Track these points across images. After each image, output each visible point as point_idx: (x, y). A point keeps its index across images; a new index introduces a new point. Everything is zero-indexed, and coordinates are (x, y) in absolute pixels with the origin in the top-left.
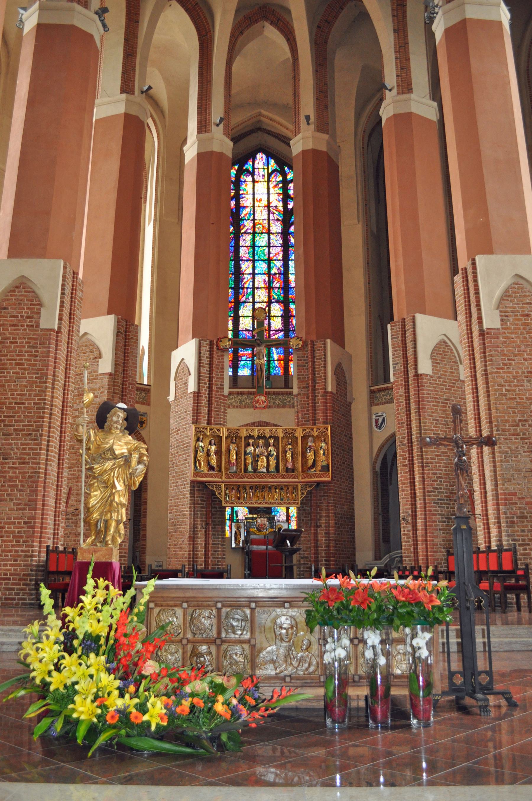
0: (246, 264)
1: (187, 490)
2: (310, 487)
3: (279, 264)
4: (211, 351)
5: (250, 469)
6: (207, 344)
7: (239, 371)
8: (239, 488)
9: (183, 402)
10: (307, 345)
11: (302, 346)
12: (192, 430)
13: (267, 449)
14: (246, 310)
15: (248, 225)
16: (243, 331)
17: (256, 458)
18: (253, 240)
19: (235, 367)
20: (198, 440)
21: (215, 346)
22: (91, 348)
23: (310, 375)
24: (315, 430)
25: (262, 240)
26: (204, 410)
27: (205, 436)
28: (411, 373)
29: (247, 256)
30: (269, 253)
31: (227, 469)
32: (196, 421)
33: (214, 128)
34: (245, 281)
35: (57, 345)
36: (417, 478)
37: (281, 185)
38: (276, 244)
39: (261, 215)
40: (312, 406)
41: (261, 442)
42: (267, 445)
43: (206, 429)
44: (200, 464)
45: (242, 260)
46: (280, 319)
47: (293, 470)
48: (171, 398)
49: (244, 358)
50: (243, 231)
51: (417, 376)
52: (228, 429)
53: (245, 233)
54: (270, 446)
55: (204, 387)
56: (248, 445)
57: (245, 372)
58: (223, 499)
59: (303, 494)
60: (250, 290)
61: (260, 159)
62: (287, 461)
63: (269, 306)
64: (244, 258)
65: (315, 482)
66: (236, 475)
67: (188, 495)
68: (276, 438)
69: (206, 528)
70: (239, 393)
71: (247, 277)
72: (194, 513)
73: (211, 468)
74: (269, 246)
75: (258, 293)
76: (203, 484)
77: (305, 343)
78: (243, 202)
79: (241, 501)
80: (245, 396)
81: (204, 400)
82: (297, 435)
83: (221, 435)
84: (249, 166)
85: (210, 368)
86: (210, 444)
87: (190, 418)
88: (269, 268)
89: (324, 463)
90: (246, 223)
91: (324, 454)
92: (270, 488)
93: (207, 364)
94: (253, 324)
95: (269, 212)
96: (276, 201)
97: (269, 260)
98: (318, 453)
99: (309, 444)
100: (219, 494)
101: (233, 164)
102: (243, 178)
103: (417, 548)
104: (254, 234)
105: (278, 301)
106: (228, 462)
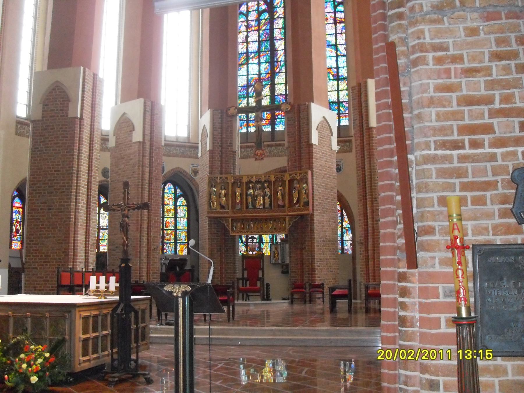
0: (279, 42)
2: (295, 218)
5: (250, 206)
6: (219, 113)
7: (276, 127)
8: (243, 220)
10: (294, 108)
11: (291, 109)
13: (263, 191)
16: (278, 95)
17: (254, 198)
21: (225, 115)
22: (128, 124)
23: (297, 132)
24: (298, 174)
29: (280, 35)
31: (233, 207)
34: (278, 56)
35: (80, 128)
40: (298, 156)
41: (258, 186)
42: (263, 188)
43: (217, 178)
44: (213, 204)
45: (276, 39)
47: (283, 206)
49: (280, 116)
52: (234, 177)
54: (265, 188)
55: (216, 146)
56: (248, 188)
58: (230, 230)
59: (290, 224)
60: (282, 63)
62: (278, 199)
64: (278, 38)
65: (298, 215)
67: (207, 227)
68: (269, 182)
73: (222, 207)
77: (292, 107)
79: (245, 231)
80: (273, 148)
81: (217, 156)
82: (285, 179)
83: (229, 181)
85: (221, 131)
86: (221, 189)
89: (306, 200)
91: (305, 193)
93: (219, 128)
94: (286, 89)
98: (301, 192)
99: (295, 186)
100: (228, 226)
103: (368, 264)
106: (234, 203)
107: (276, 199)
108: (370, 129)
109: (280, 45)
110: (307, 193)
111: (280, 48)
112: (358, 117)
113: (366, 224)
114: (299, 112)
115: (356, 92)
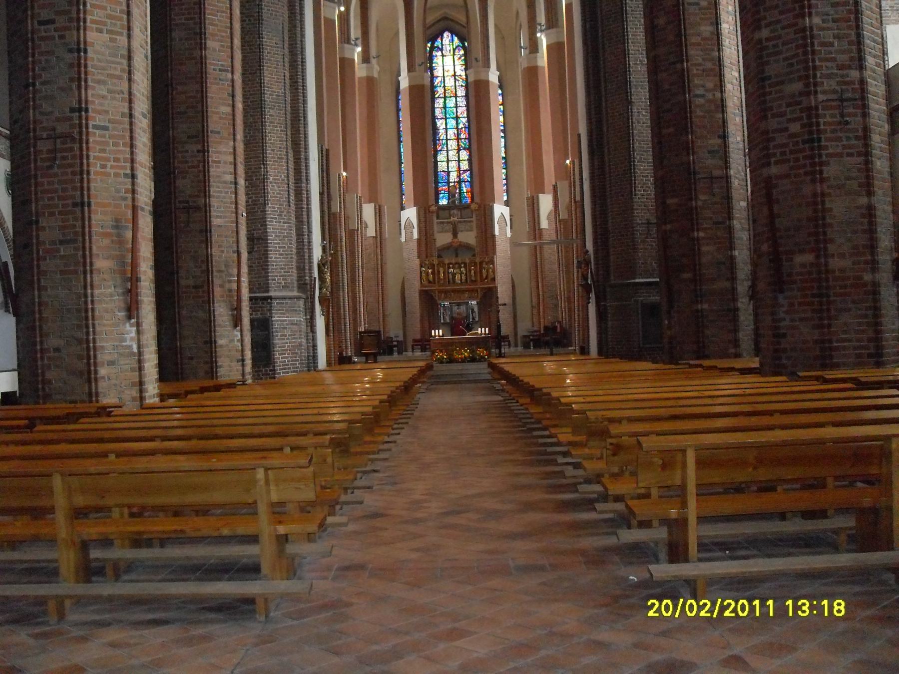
0: (441, 121)
1: (417, 295)
3: (464, 120)
4: (425, 213)
8: (446, 292)
9: (411, 244)
12: (417, 262)
14: (441, 157)
15: (440, 91)
17: (454, 275)
18: (445, 103)
19: (437, 199)
20: (421, 266)
25: (451, 103)
27: (425, 264)
28: (537, 228)
30: (457, 112)
32: (419, 257)
33: (417, 68)
36: (540, 285)
37: (463, 58)
38: (461, 105)
39: (450, 82)
41: (457, 266)
46: (467, 162)
47: (475, 281)
48: (403, 239)
50: (436, 96)
53: (438, 97)
56: (449, 268)
57: (443, 202)
60: (444, 141)
63: (458, 152)
66: (443, 285)
68: (465, 264)
71: (442, 132)
74: (456, 107)
75: (450, 143)
76: (426, 291)
77: (480, 206)
78: (436, 73)
87: (416, 254)
88: (457, 124)
90: (438, 89)
92: (463, 291)
95: (455, 79)
96: (460, 71)
97: (457, 118)
104: (445, 97)
105: (464, 149)
106: (439, 278)
107: (471, 276)
108: (540, 230)
109: (441, 124)
110: (494, 272)
111: (441, 127)
113: (539, 295)
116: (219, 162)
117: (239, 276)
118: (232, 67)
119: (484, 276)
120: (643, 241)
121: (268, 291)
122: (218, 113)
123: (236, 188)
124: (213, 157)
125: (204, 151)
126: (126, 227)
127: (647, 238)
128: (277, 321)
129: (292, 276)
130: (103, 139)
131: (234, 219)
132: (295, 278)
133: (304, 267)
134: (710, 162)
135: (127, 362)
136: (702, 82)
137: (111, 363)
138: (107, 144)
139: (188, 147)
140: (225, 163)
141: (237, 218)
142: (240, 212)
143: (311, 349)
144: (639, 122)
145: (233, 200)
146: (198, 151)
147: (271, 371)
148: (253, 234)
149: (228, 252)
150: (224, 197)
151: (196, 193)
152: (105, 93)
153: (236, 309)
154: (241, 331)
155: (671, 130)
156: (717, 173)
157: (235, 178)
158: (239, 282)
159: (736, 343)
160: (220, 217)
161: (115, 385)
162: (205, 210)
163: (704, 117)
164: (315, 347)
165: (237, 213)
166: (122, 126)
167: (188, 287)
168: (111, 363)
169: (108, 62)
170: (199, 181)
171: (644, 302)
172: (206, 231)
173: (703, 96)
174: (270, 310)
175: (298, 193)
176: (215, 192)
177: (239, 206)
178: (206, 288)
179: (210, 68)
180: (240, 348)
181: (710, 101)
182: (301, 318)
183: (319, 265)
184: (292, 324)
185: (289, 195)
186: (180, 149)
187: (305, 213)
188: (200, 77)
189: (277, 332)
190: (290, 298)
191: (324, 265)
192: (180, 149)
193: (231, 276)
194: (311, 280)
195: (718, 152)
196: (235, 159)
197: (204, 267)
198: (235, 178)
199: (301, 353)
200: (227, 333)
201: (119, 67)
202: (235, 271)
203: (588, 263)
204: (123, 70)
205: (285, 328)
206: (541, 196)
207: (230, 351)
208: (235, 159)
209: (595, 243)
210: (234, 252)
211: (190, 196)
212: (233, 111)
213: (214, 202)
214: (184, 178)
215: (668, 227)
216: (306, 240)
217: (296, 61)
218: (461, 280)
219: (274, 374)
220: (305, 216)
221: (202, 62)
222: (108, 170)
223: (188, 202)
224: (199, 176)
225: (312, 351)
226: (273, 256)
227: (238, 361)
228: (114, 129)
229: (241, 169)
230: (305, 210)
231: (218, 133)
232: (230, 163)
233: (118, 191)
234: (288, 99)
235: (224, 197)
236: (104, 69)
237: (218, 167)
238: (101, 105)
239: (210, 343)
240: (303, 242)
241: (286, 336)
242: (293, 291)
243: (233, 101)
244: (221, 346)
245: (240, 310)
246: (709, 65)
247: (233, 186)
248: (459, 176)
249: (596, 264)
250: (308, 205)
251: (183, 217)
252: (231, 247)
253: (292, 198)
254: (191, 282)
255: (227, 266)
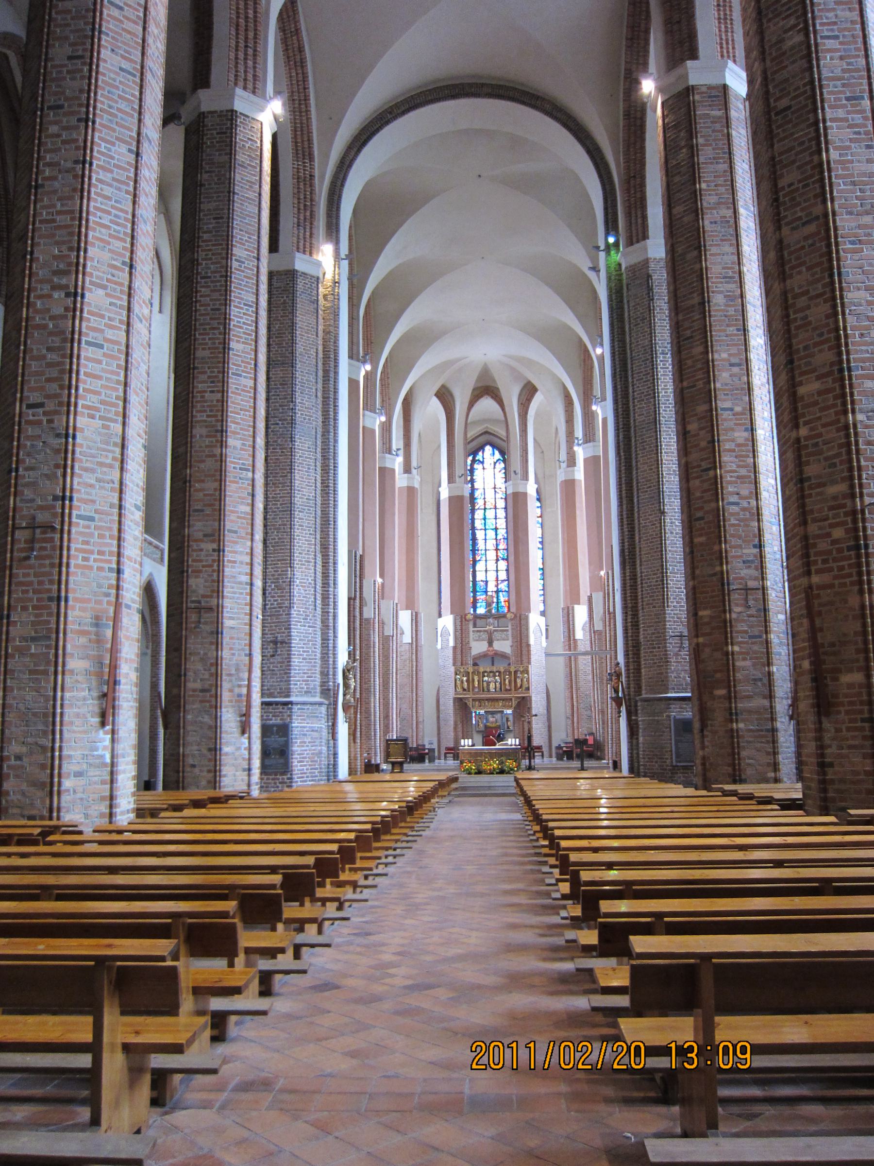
1: (451, 702)
4: (461, 621)
12: (452, 669)
14: (480, 566)
15: (480, 503)
17: (488, 683)
19: (475, 608)
20: (456, 674)
25: (490, 514)
26: (459, 657)
32: (454, 664)
41: (491, 674)
47: (510, 690)
48: (439, 646)
51: (575, 640)
56: (484, 676)
57: (481, 610)
60: (483, 552)
61: (488, 449)
66: (478, 693)
68: (500, 672)
69: (462, 722)
70: (478, 631)
72: (455, 714)
76: (461, 699)
77: (515, 616)
78: (476, 485)
84: (479, 457)
87: (451, 661)
88: (496, 535)
101: (469, 455)
102: (476, 466)
105: (503, 559)
108: (575, 641)
112: (566, 630)
113: (573, 705)
114: (520, 620)
115: (566, 611)
116: (235, 562)
117: (249, 680)
118: (254, 466)
119: (519, 685)
120: (677, 655)
121: (288, 696)
122: (237, 512)
123: (251, 589)
124: (228, 556)
125: (219, 550)
126: (107, 626)
127: (680, 651)
128: (297, 727)
129: (315, 681)
130: (87, 531)
131: (248, 621)
132: (318, 683)
133: (328, 671)
134: (744, 572)
135: (97, 773)
136: (736, 489)
137: (79, 774)
138: (91, 535)
139: (203, 546)
140: (241, 563)
141: (251, 620)
142: (254, 614)
143: (332, 757)
144: (672, 533)
145: (248, 601)
146: (214, 550)
147: (288, 779)
148: (277, 637)
149: (239, 655)
150: (238, 598)
151: (209, 594)
152: (93, 482)
153: (244, 715)
154: (249, 738)
155: (702, 539)
156: (751, 584)
157: (251, 579)
158: (249, 686)
159: (775, 767)
160: (232, 618)
161: (82, 799)
162: (216, 611)
163: (739, 525)
164: (335, 755)
165: (251, 615)
166: (109, 517)
167: (194, 690)
168: (79, 774)
169: (98, 449)
170: (213, 581)
171: (678, 717)
172: (217, 632)
173: (737, 504)
174: (290, 716)
175: (325, 598)
176: (228, 592)
177: (254, 608)
178: (213, 692)
179: (230, 467)
180: (247, 757)
181: (744, 509)
182: (322, 725)
183: (344, 671)
184: (313, 731)
185: (315, 599)
186: (195, 547)
187: (331, 618)
188: (219, 475)
189: (296, 738)
190: (312, 704)
191: (349, 671)
192: (195, 547)
193: (243, 680)
194: (334, 686)
195: (752, 562)
196: (252, 559)
197: (213, 670)
198: (251, 579)
199: (321, 761)
200: (234, 740)
201: (110, 455)
202: (246, 675)
203: (619, 675)
204: (114, 459)
205: (305, 735)
206: (576, 607)
207: (236, 759)
208: (252, 559)
209: (626, 655)
210: (246, 655)
211: (203, 596)
212: (253, 510)
213: (227, 603)
214: (197, 577)
215: (701, 640)
216: (331, 645)
217: (328, 466)
218: (495, 688)
219: (291, 782)
220: (331, 621)
221: (221, 460)
222: (91, 563)
223: (199, 602)
224: (212, 575)
225: (332, 759)
226: (296, 661)
227: (244, 770)
228: (100, 520)
229: (258, 571)
230: (331, 614)
231: (236, 532)
232: (247, 564)
233: (100, 586)
234: (319, 502)
235: (238, 598)
236: (94, 457)
237: (232, 567)
238: (88, 494)
239: (215, 750)
240: (328, 647)
241: (305, 742)
242: (315, 696)
243: (253, 500)
244: (227, 754)
245: (249, 716)
246: (743, 472)
247: (248, 587)
248: (497, 586)
249: (628, 677)
250: (334, 609)
251: (193, 617)
252: (243, 650)
253: (319, 602)
254: (198, 685)
255: (238, 670)
